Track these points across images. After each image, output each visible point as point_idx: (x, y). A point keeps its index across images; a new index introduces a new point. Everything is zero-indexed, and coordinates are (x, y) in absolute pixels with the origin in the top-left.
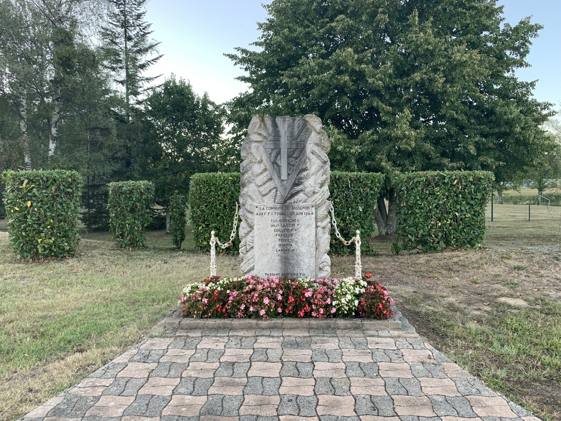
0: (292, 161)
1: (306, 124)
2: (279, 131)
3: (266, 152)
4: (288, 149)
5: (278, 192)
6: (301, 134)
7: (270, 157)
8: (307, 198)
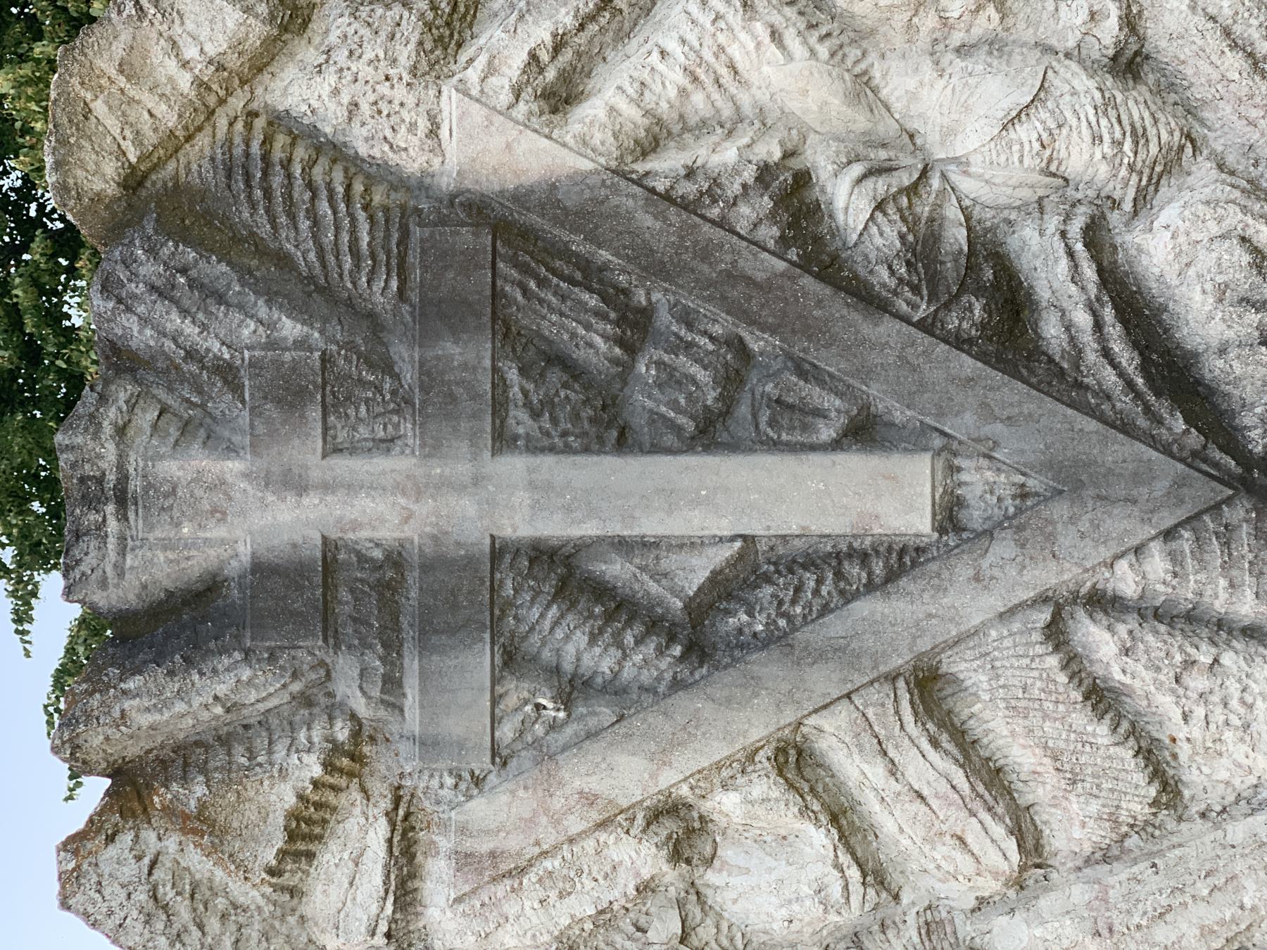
0: (671, 378)
1: (176, 189)
2: (261, 569)
3: (545, 755)
4: (503, 441)
5: (1125, 580)
6: (305, 256)
7: (614, 690)
8: (1203, 171)
